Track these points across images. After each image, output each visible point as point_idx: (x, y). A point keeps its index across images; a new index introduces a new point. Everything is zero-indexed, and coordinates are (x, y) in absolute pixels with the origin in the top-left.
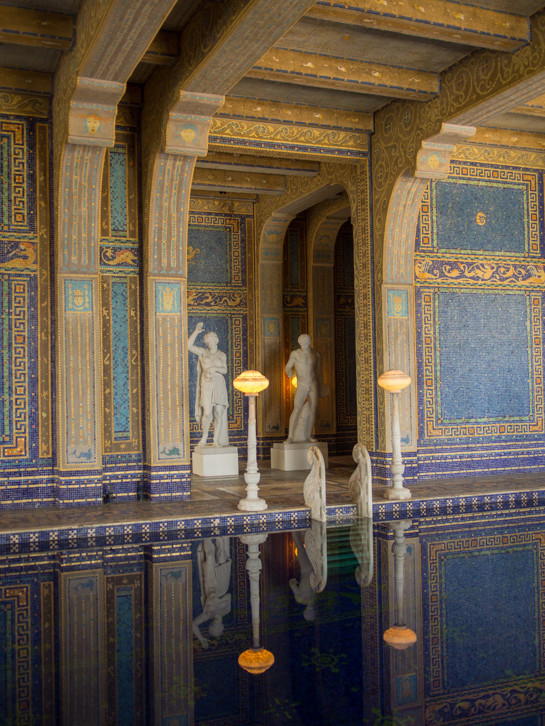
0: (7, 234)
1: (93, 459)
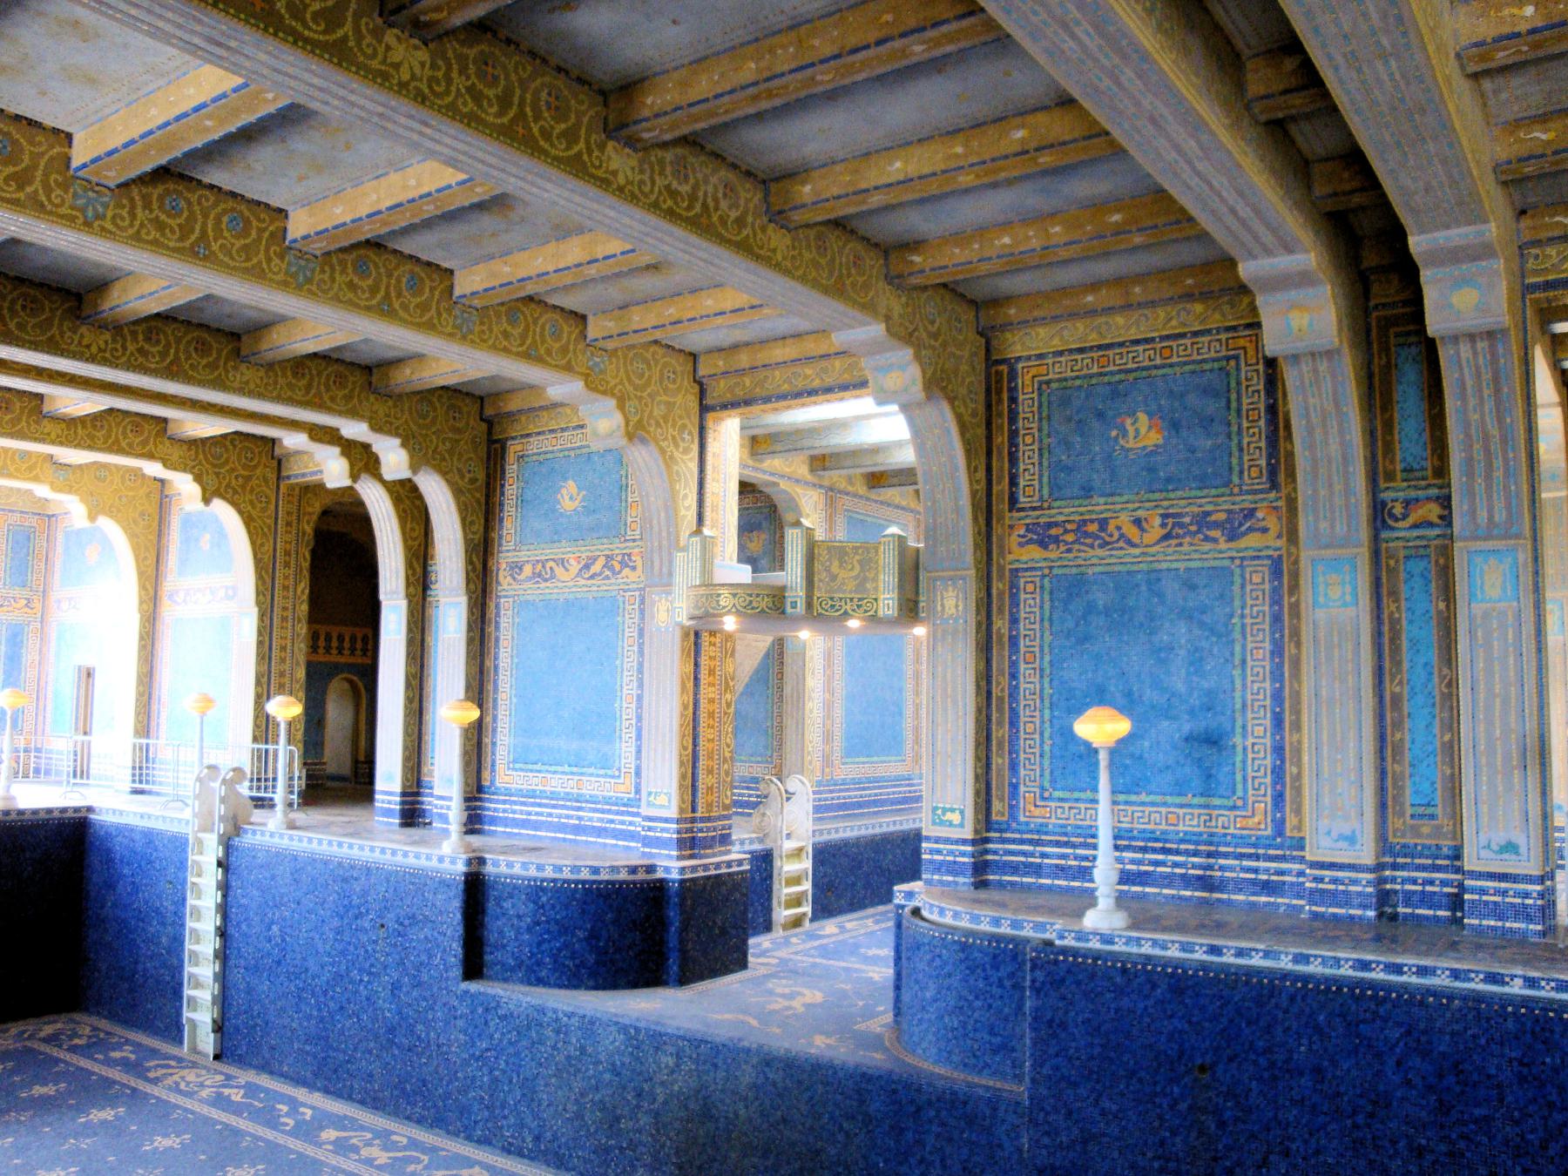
0: (1238, 499)
1: (1358, 847)
